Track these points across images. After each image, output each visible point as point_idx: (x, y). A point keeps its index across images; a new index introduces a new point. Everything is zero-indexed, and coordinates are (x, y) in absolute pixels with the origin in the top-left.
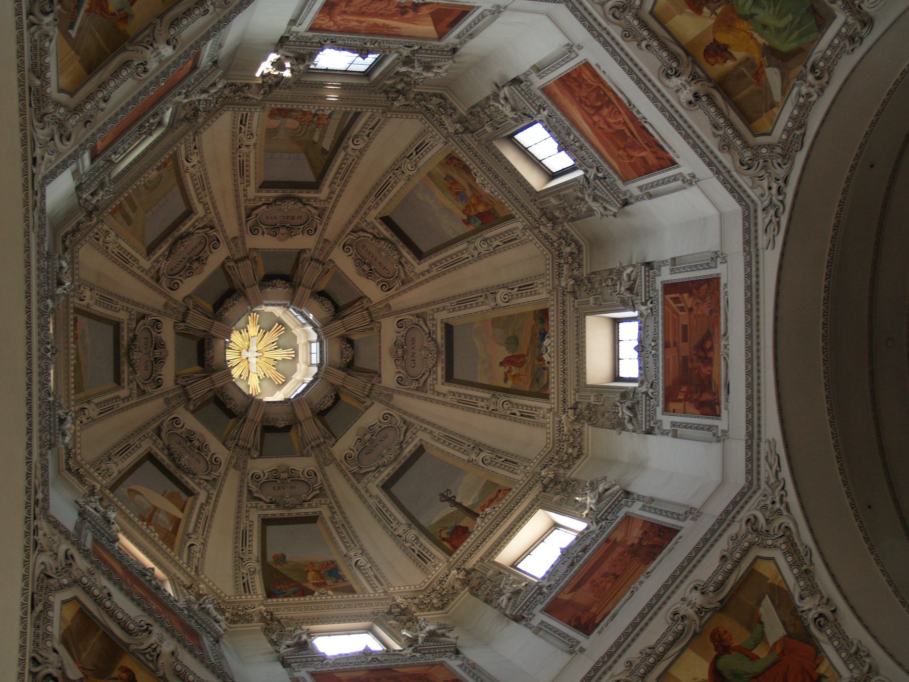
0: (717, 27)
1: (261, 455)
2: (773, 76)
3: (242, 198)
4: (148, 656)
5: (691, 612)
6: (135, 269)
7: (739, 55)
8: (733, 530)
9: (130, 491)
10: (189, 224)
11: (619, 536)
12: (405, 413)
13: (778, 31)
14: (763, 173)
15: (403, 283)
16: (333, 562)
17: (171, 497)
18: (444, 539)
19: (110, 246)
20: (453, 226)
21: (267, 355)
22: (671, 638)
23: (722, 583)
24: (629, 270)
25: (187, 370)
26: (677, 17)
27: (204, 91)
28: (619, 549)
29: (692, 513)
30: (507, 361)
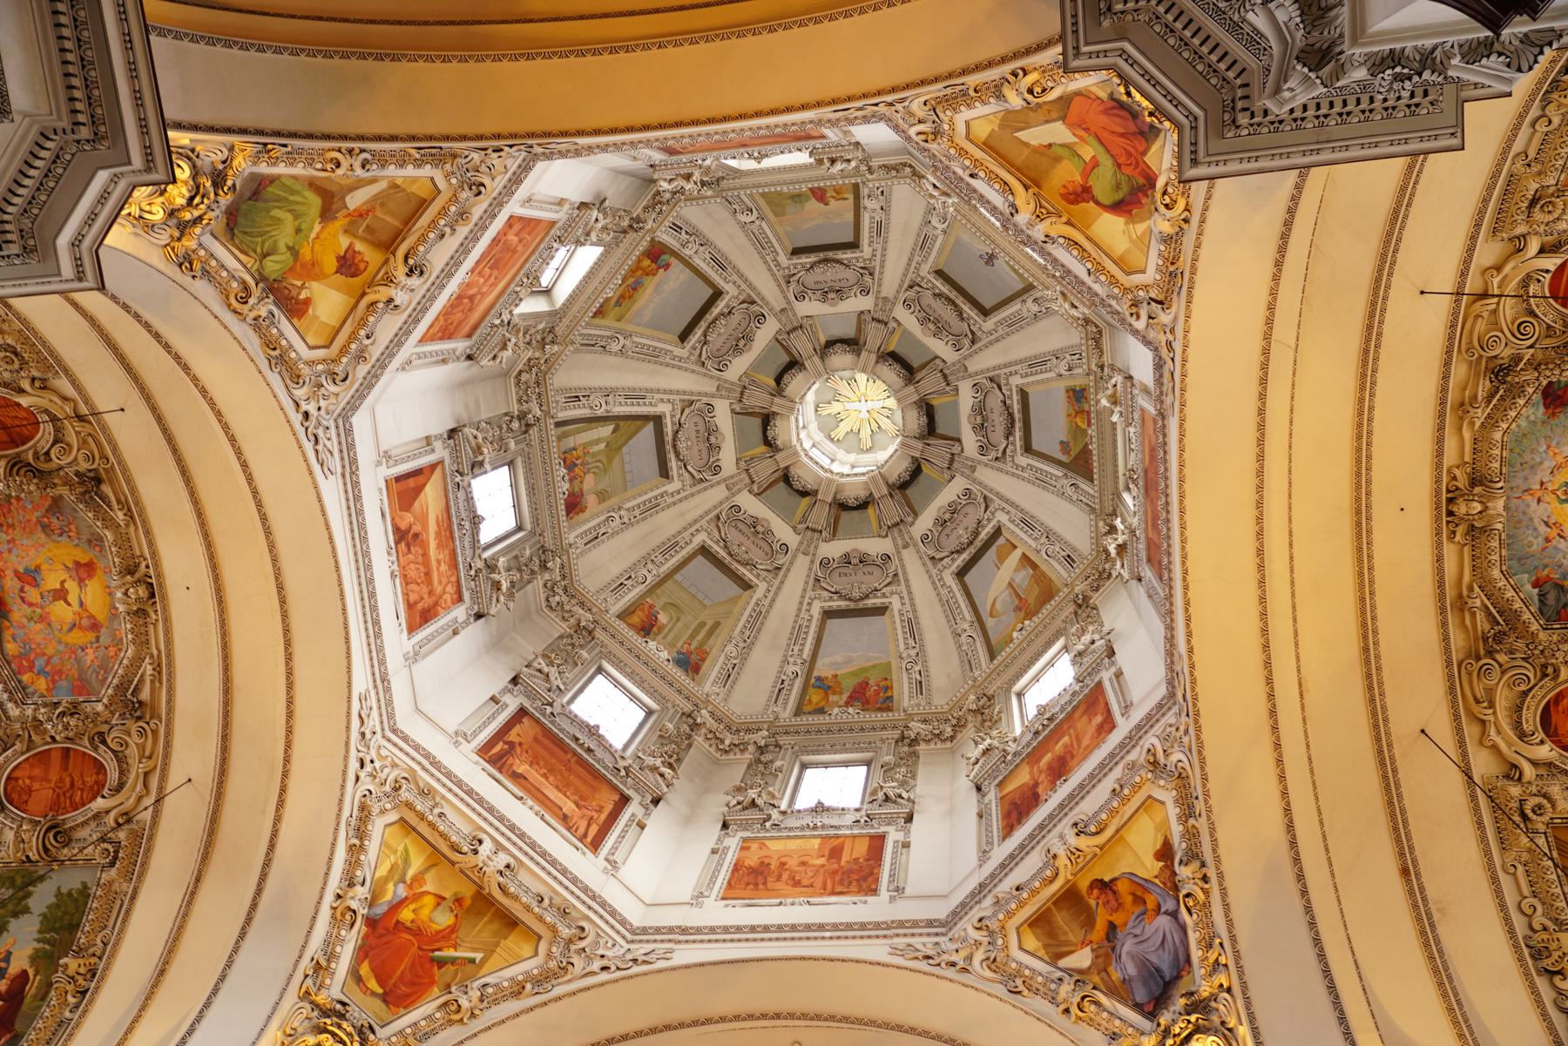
0: (318, 277)
15: (753, 302)
17: (1001, 558)
19: (742, 645)
21: (863, 389)
22: (1075, 253)
27: (547, 675)
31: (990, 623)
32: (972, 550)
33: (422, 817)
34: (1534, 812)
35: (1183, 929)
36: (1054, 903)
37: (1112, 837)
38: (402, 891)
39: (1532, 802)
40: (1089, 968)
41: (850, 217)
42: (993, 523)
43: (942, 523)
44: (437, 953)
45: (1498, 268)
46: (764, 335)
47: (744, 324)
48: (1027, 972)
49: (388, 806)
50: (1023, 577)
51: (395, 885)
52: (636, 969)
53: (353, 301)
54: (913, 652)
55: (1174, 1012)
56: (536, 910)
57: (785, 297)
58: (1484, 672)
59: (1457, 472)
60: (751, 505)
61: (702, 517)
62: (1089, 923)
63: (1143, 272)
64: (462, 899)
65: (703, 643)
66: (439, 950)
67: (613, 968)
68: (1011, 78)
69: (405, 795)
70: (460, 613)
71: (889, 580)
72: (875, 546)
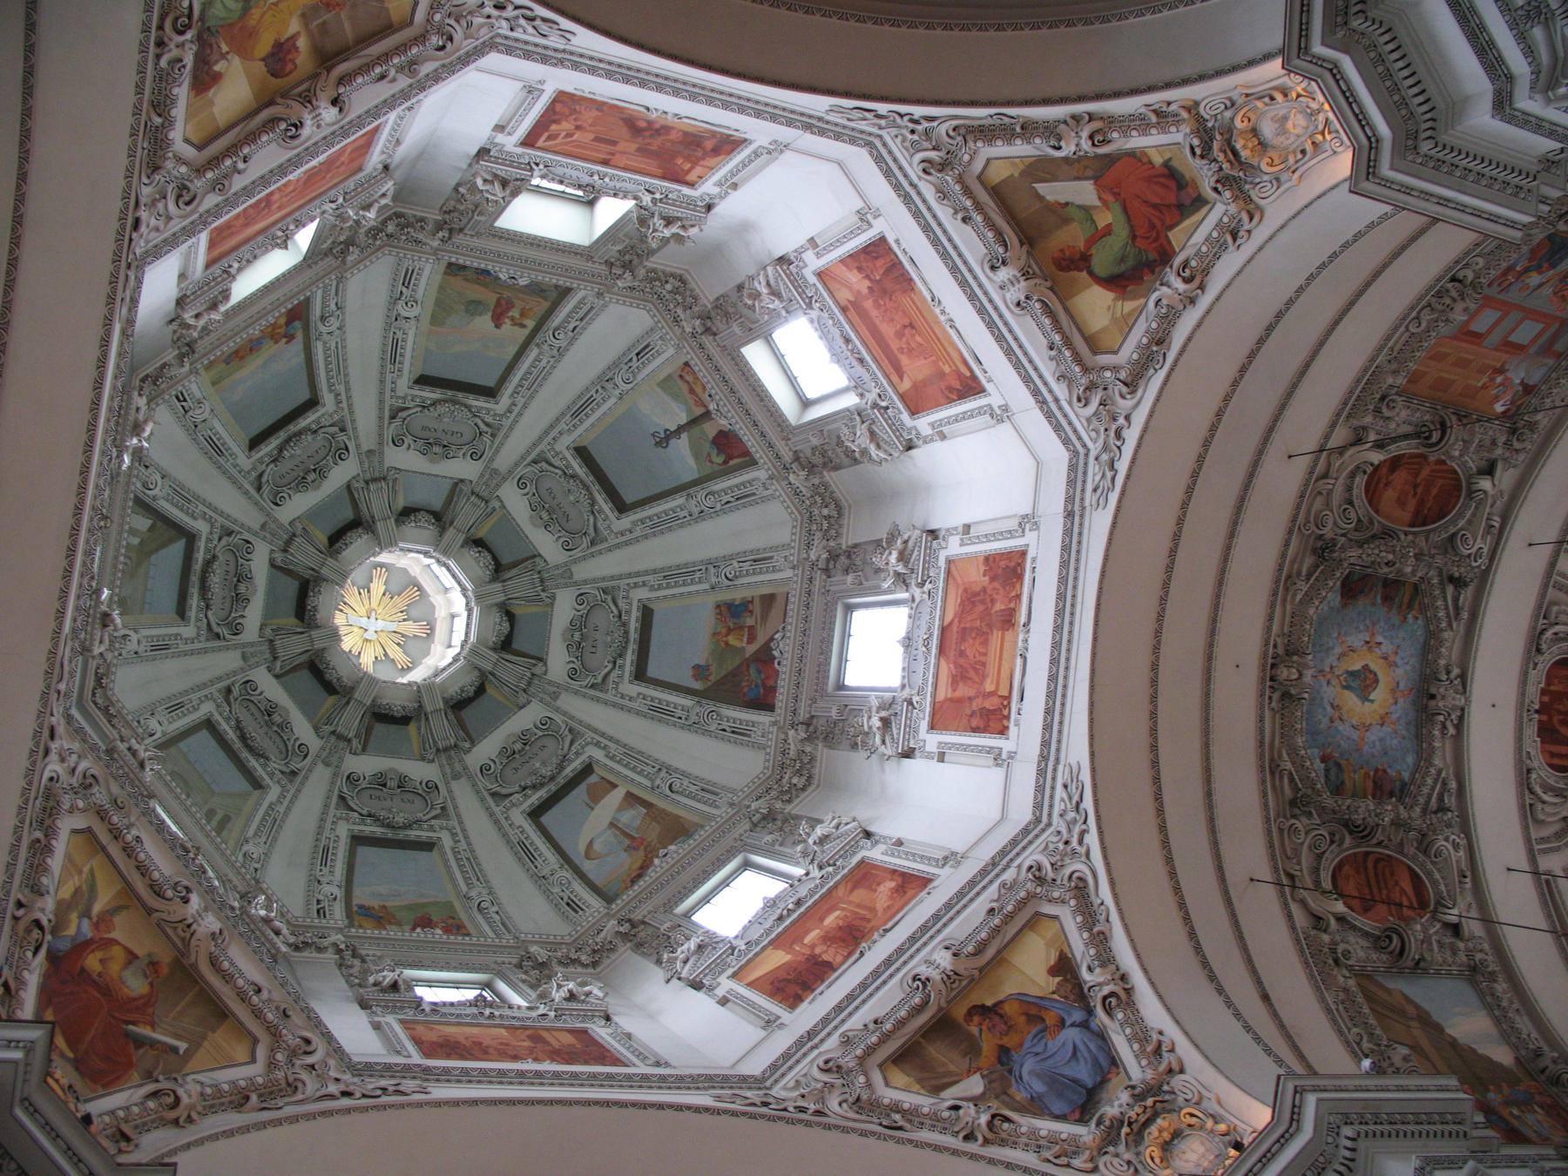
0: (244, 54)
4: (954, 986)
15: (343, 430)
16: (718, 606)
17: (595, 797)
18: (725, 462)
21: (374, 604)
22: (1047, 321)
23: (999, 235)
30: (498, 320)
31: (588, 866)
32: (553, 787)
33: (116, 835)
34: (1344, 956)
35: (1102, 1036)
36: (923, 1036)
37: (993, 959)
38: (87, 930)
39: (1341, 948)
40: (984, 1094)
41: (511, 351)
42: (583, 758)
43: (508, 754)
44: (131, 1027)
45: (1341, 450)
46: (341, 474)
47: (323, 452)
48: (906, 1106)
49: (81, 804)
50: (632, 818)
51: (80, 917)
52: (385, 1099)
53: (255, 105)
55: (1121, 1106)
56: (255, 999)
57: (380, 435)
58: (1293, 830)
59: (1279, 640)
60: (270, 688)
61: (212, 682)
62: (973, 1049)
64: (157, 963)
66: (134, 1023)
67: (358, 1095)
68: (1070, 121)
69: (99, 795)
71: (434, 813)
72: (419, 771)
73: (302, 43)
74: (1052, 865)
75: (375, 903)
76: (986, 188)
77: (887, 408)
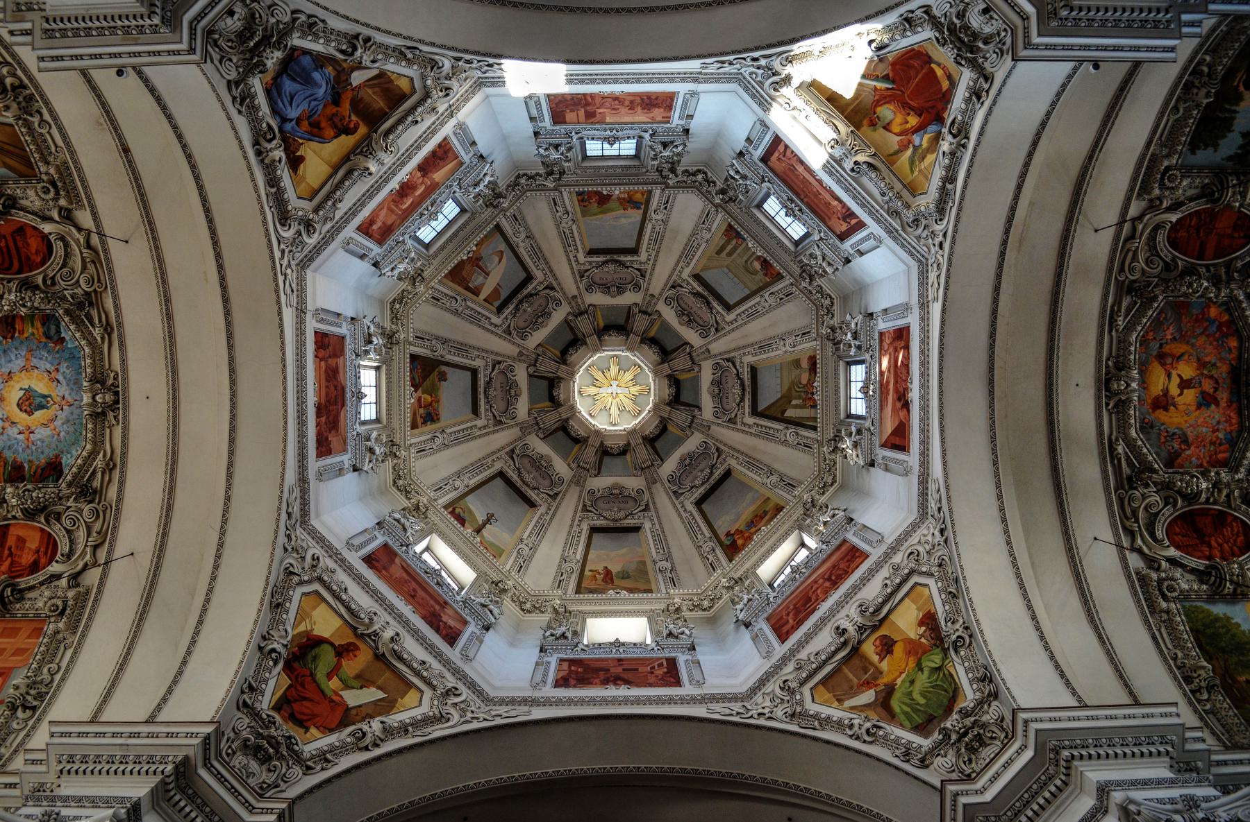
0: (909, 641)
1: (530, 376)
2: (868, 696)
3: (741, 352)
5: (376, 627)
6: (681, 264)
7: (884, 665)
8: (448, 675)
9: (502, 252)
10: (719, 309)
11: (449, 611)
12: (564, 495)
13: (910, 694)
14: (778, 701)
15: (675, 492)
17: (496, 292)
18: (454, 509)
20: (726, 523)
21: (614, 401)
22: (353, 606)
23: (400, 659)
24: (687, 632)
25: (600, 316)
26: (914, 607)
27: (824, 259)
28: (437, 608)
29: (467, 659)
30: (608, 573)
31: (503, 246)
38: (916, 139)
51: (921, 145)
54: (564, 225)
63: (303, 594)
65: (728, 242)
70: (882, 325)
73: (875, 658)
74: (300, 235)
75: (630, 211)
76: (416, 686)
77: (402, 545)
